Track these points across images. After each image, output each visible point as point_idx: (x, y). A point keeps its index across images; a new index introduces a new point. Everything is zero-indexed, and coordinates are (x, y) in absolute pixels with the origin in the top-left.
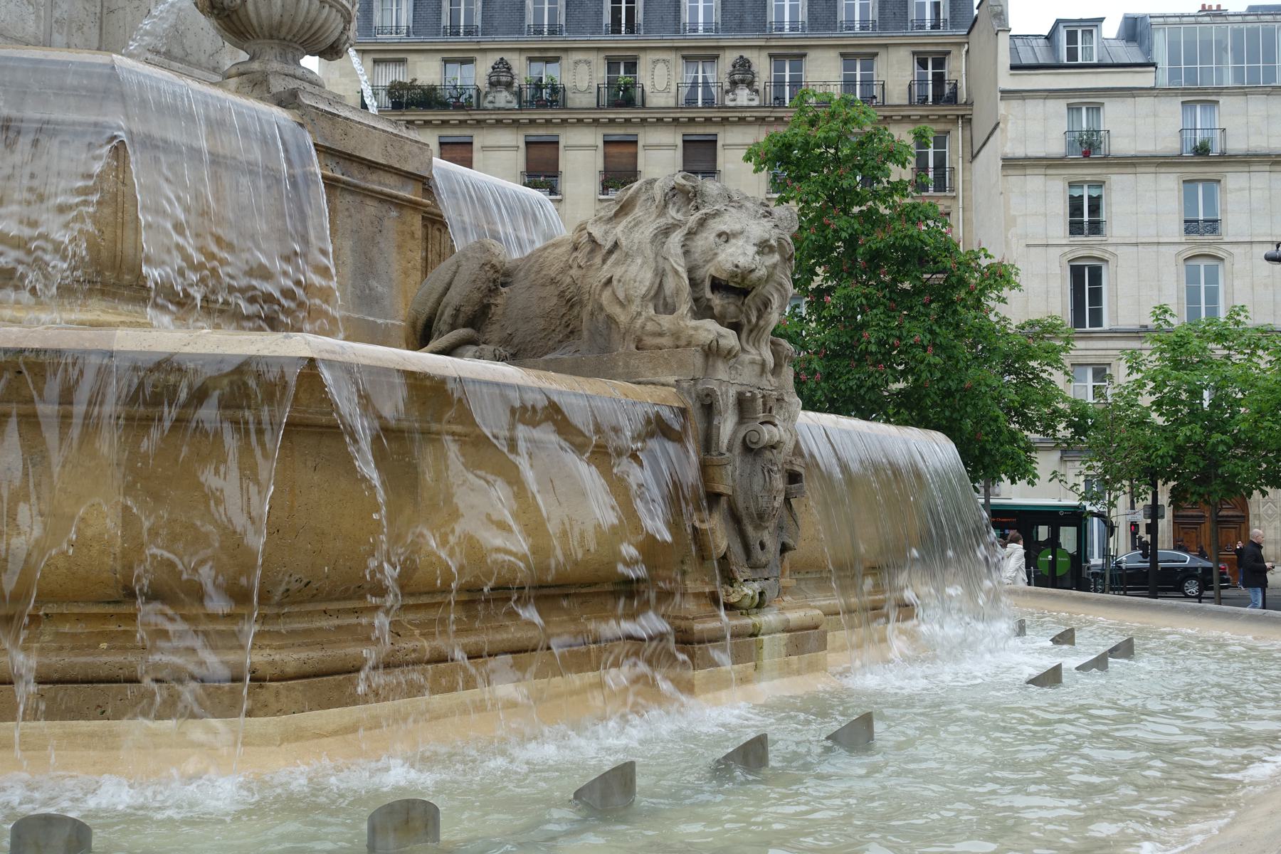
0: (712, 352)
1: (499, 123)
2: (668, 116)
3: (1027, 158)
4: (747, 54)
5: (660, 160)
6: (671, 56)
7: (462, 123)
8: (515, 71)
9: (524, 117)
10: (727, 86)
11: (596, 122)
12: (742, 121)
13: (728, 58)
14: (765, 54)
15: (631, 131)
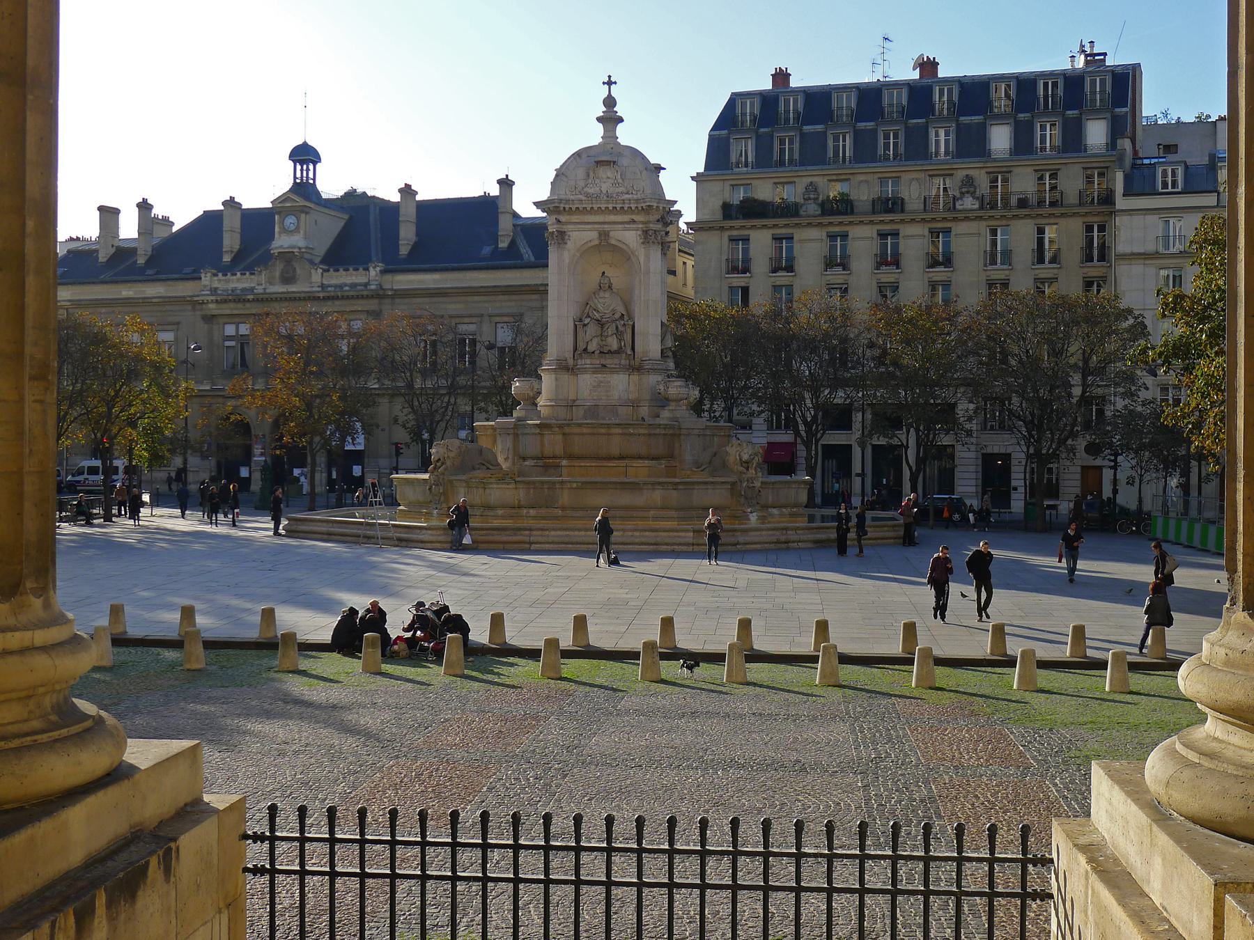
1: (809, 225)
3: (1133, 254)
4: (970, 172)
5: (914, 242)
6: (922, 175)
7: (786, 226)
8: (820, 190)
10: (957, 194)
11: (872, 222)
13: (960, 174)
14: (983, 171)
15: (895, 227)
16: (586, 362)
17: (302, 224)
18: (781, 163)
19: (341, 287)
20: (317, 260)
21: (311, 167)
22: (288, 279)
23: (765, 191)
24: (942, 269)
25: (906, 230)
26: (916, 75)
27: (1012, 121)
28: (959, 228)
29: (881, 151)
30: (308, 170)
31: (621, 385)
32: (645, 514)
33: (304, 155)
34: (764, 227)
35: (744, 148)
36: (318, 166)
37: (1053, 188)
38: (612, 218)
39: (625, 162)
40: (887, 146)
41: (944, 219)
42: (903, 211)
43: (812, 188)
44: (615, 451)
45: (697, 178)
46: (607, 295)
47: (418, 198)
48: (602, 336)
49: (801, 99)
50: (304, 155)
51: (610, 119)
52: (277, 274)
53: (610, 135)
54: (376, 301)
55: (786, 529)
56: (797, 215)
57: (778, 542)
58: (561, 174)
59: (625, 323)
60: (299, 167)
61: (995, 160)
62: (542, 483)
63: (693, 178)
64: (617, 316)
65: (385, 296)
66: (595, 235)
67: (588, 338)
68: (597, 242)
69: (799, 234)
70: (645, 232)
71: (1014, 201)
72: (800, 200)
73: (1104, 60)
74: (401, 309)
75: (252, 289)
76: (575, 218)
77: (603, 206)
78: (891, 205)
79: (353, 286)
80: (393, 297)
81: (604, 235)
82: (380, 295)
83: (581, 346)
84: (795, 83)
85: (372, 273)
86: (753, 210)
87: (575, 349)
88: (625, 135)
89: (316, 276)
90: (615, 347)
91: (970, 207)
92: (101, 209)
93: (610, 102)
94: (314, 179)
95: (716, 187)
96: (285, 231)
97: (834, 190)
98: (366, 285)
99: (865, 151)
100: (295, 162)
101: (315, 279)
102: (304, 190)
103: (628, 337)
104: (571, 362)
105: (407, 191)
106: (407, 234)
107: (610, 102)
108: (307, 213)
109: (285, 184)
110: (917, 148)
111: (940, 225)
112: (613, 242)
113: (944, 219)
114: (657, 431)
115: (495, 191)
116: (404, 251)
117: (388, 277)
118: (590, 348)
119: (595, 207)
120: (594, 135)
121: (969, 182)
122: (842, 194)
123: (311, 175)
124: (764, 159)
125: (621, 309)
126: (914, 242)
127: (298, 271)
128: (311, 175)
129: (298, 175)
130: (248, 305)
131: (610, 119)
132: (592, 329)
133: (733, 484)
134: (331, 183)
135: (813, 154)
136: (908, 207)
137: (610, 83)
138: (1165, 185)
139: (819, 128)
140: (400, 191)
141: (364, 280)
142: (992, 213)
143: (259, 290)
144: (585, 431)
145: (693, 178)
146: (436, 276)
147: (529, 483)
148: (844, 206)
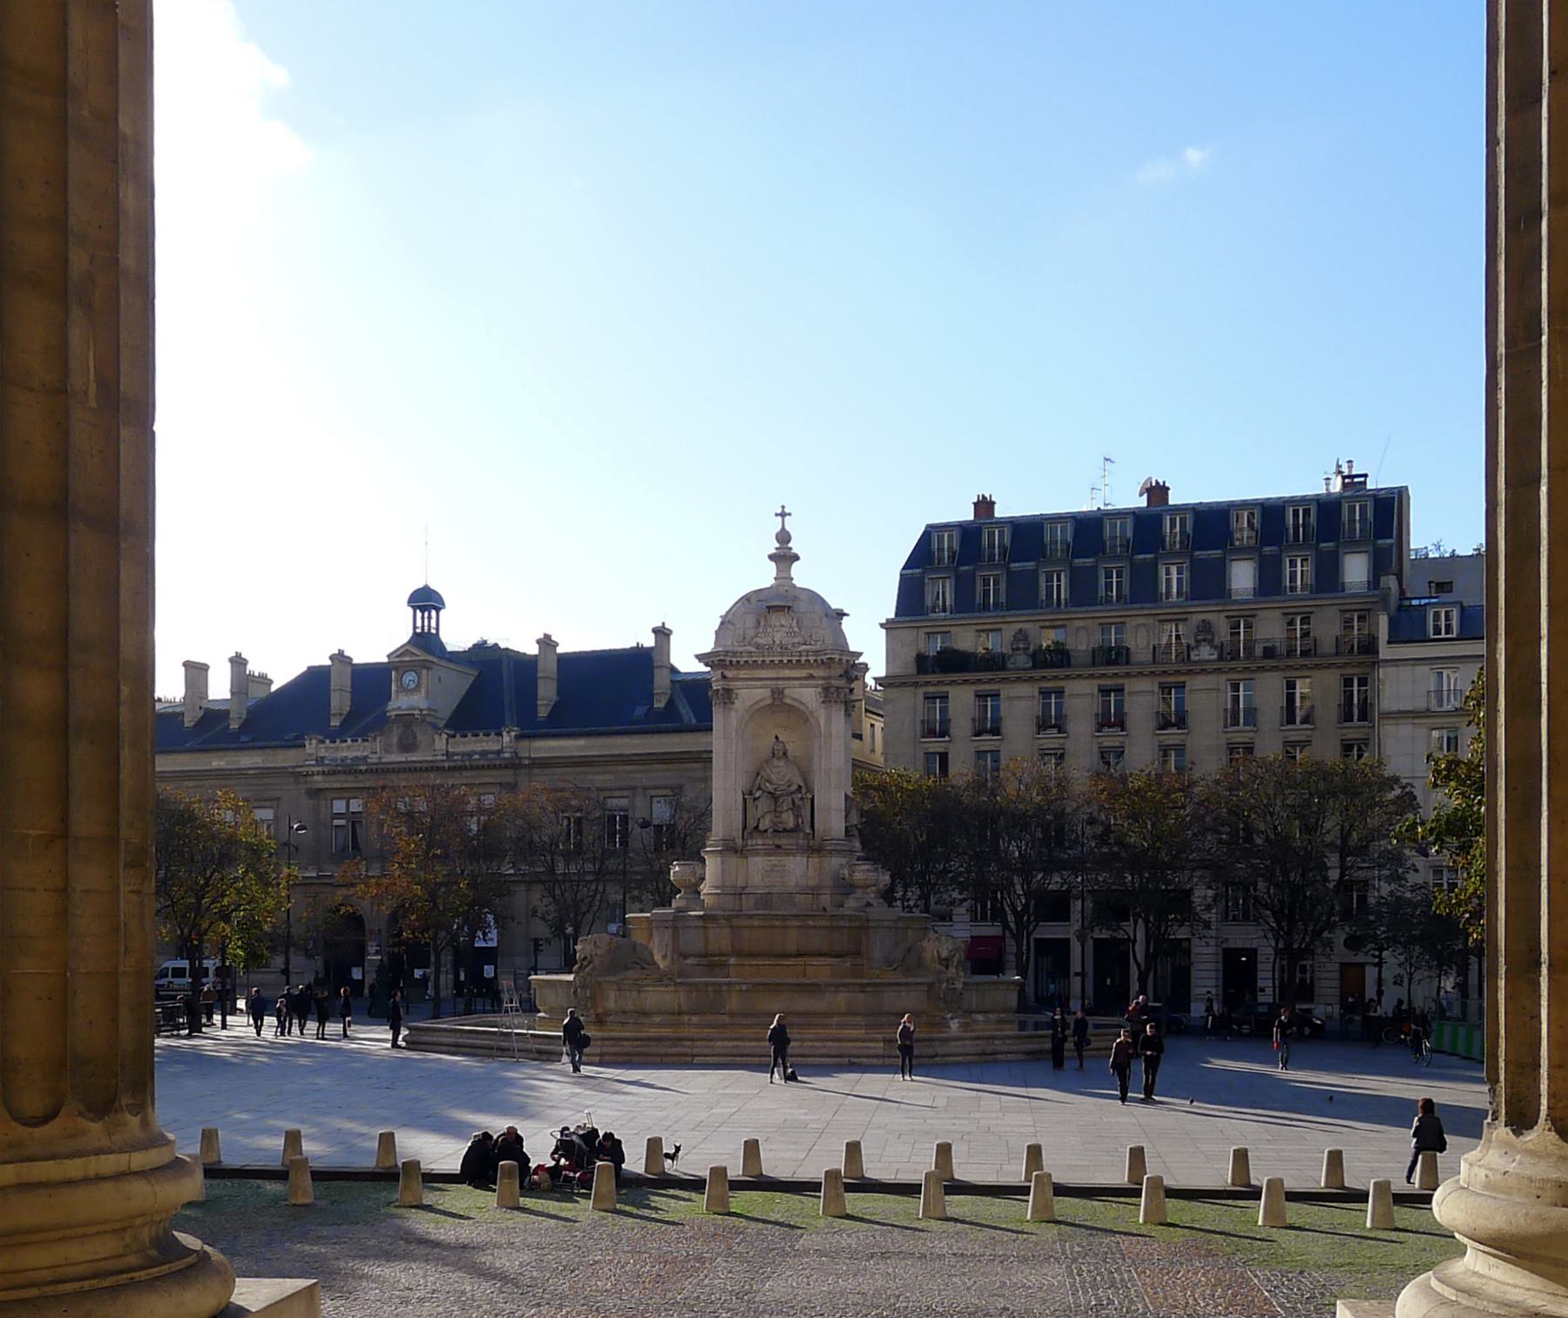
0: (940, 972)
1: (1019, 679)
2: (1146, 670)
5: (1142, 700)
6: (1150, 621)
7: (990, 681)
9: (1038, 674)
10: (1193, 643)
11: (1092, 676)
12: (1203, 671)
13: (1196, 619)
15: (1120, 681)
16: (758, 842)
17: (424, 681)
18: (985, 607)
19: (470, 754)
20: (442, 724)
21: (434, 613)
22: (408, 746)
23: (967, 640)
24: (1174, 730)
25: (1131, 685)
26: (1143, 502)
27: (1256, 556)
28: (1195, 683)
29: (1102, 592)
30: (430, 618)
31: (797, 869)
32: (829, 1021)
33: (426, 601)
34: (966, 682)
35: (942, 590)
36: (442, 613)
37: (1305, 634)
38: (787, 673)
39: (802, 606)
40: (1109, 586)
41: (1178, 672)
42: (1128, 663)
43: (1021, 636)
44: (792, 948)
45: (888, 626)
46: (782, 763)
47: (559, 650)
48: (776, 812)
49: (1007, 532)
50: (426, 601)
51: (784, 557)
52: (395, 740)
53: (784, 576)
54: (510, 772)
55: (994, 1038)
56: (1003, 668)
57: (983, 1054)
58: (726, 622)
59: (802, 797)
60: (419, 614)
61: (1237, 602)
62: (706, 984)
63: (882, 625)
64: (793, 788)
65: (521, 766)
66: (766, 693)
67: (759, 814)
68: (769, 701)
69: (1006, 691)
70: (826, 689)
71: (1259, 651)
72: (1007, 650)
73: (1365, 483)
74: (540, 781)
75: (366, 758)
76: (743, 674)
77: (777, 659)
78: (1113, 656)
79: (483, 754)
80: (531, 766)
81: (778, 694)
82: (514, 764)
83: (751, 823)
84: (999, 512)
85: (506, 739)
86: (952, 663)
87: (745, 828)
88: (802, 576)
89: (441, 743)
90: (791, 824)
91: (1207, 657)
92: (187, 664)
93: (784, 537)
94: (437, 629)
95: (909, 635)
96: (403, 689)
97: (1048, 639)
98: (499, 752)
99: (1084, 593)
100: (415, 608)
101: (439, 746)
102: (425, 641)
103: (806, 812)
104: (739, 842)
105: (546, 643)
106: (547, 693)
107: (784, 537)
108: (429, 669)
109: (403, 635)
110: (1144, 590)
111: (1172, 679)
112: (788, 701)
113: (1178, 672)
114: (841, 923)
115: (649, 641)
116: (543, 712)
117: (525, 743)
118: (761, 827)
119: (768, 659)
120: (764, 576)
121: (1206, 628)
122: (1056, 643)
123: (433, 624)
124: (965, 603)
125: (799, 781)
126: (1142, 700)
127: (419, 737)
128: (433, 624)
129: (419, 624)
130: (361, 777)
131: (784, 557)
132: (764, 804)
133: (930, 985)
134: (457, 634)
135: (1022, 596)
136: (1135, 658)
137: (783, 515)
138: (1437, 630)
139: (1030, 565)
140: (538, 642)
141: (497, 747)
142: (1233, 664)
143: (373, 759)
144: (756, 923)
145: (882, 625)
146: (581, 742)
147: (690, 984)
148: (1058, 658)
